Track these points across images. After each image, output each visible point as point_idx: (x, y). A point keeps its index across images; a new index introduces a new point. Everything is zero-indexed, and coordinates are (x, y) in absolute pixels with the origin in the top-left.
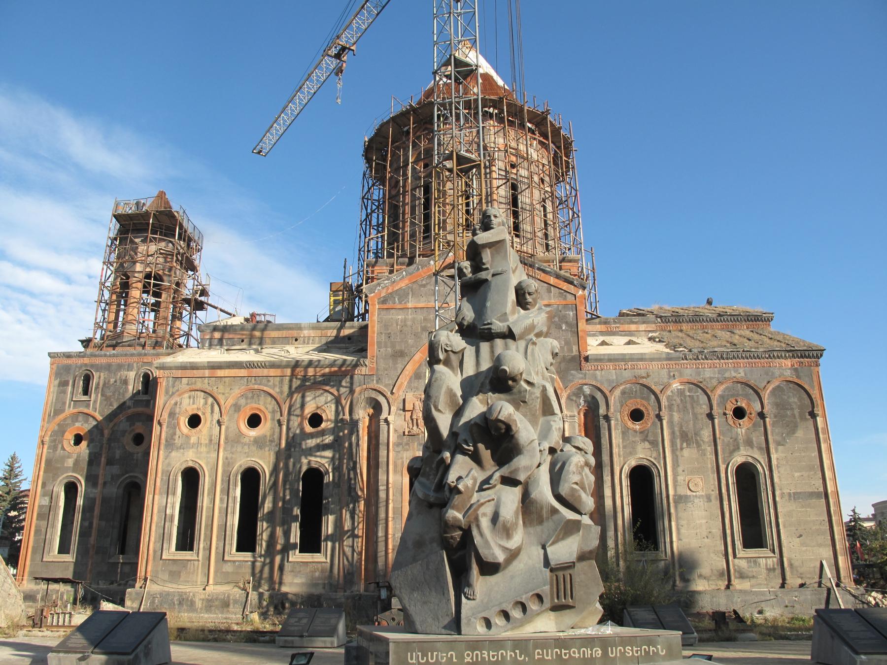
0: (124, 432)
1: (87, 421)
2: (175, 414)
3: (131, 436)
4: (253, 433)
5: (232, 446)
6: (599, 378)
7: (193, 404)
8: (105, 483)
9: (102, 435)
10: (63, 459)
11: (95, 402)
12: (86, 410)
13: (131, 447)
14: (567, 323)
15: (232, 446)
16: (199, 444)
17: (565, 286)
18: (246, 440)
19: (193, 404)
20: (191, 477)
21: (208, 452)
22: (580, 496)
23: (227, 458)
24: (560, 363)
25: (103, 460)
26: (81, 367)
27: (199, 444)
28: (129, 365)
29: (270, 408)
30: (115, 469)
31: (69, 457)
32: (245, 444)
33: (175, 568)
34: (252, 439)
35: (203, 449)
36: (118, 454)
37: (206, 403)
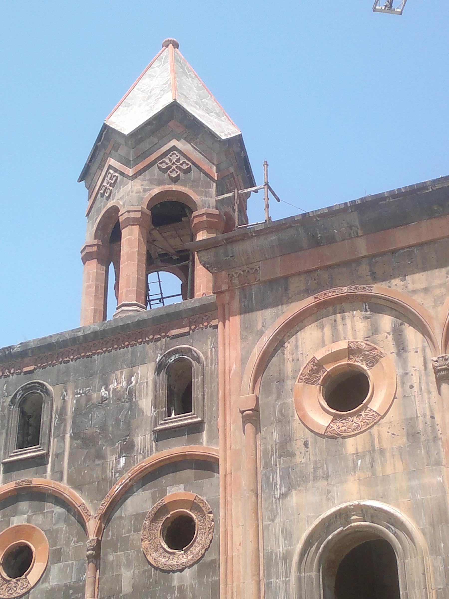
7: (335, 339)
11: (59, 456)
12: (37, 481)
21: (413, 473)
27: (374, 453)
35: (393, 467)
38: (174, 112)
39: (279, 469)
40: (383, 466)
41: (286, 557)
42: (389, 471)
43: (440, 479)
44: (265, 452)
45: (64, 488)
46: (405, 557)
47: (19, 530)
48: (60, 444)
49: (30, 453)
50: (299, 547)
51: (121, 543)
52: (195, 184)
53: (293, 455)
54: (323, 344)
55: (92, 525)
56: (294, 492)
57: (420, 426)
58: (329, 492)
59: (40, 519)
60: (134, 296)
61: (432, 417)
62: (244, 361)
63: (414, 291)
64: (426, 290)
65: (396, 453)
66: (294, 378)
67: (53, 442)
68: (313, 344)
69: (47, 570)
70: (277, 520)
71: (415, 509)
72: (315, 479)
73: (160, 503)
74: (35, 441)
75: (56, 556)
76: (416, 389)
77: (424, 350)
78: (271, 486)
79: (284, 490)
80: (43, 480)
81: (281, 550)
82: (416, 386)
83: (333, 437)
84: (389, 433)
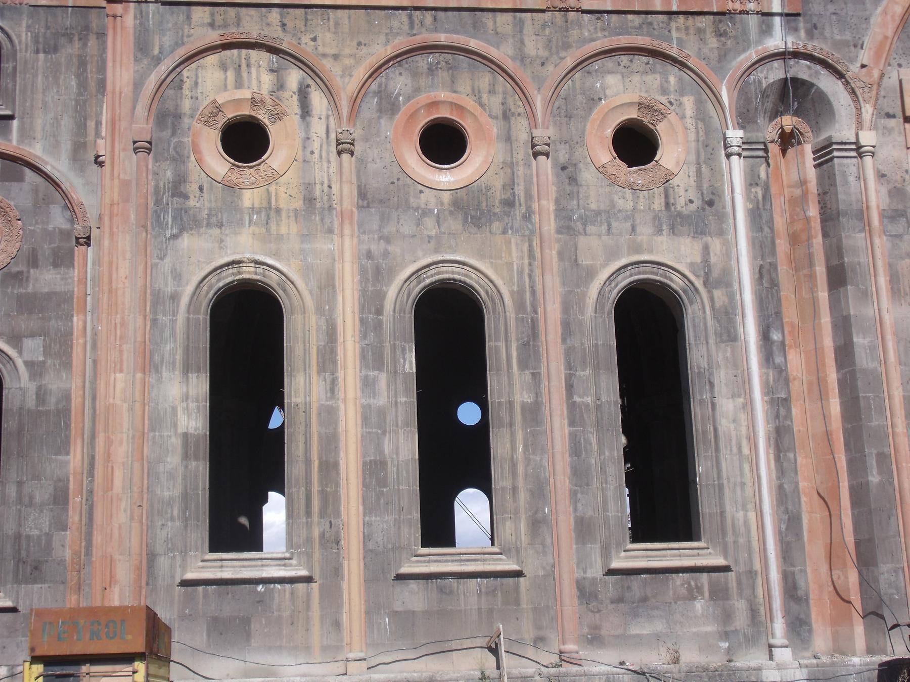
2: (178, 116)
4: (447, 178)
5: (384, 219)
7: (239, 85)
15: (384, 219)
18: (428, 197)
19: (239, 85)
21: (305, 237)
23: (369, 255)
29: (495, 103)
32: (426, 212)
33: (230, 606)
34: (446, 197)
35: (288, 228)
39: (171, 209)
40: (278, 225)
41: (175, 297)
42: (284, 230)
43: (331, 246)
44: (157, 187)
46: (292, 313)
50: (190, 289)
53: (186, 197)
56: (185, 235)
57: (318, 193)
58: (222, 241)
61: (330, 187)
62: (138, 85)
63: (324, 55)
64: (336, 57)
65: (292, 214)
66: (192, 117)
68: (220, 88)
70: (167, 260)
71: (307, 270)
72: (209, 225)
76: (316, 155)
77: (328, 117)
78: (160, 224)
79: (175, 231)
81: (170, 289)
82: (317, 152)
83: (231, 188)
84: (287, 195)
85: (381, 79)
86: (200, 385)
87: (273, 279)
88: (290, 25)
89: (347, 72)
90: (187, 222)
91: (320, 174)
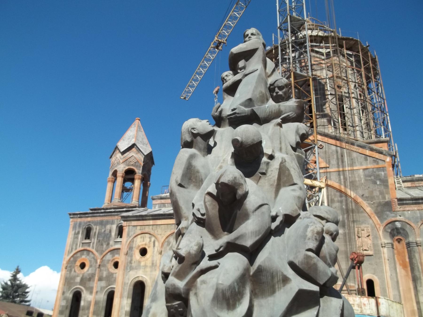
0: (109, 261)
1: (88, 255)
3: (113, 263)
6: (407, 216)
7: (143, 241)
8: (97, 292)
9: (96, 262)
10: (74, 278)
11: (93, 243)
12: (88, 248)
13: (112, 269)
14: (380, 180)
16: (145, 266)
17: (377, 155)
19: (143, 241)
20: (139, 288)
21: (151, 271)
22: (315, 265)
24: (377, 207)
25: (96, 278)
26: (87, 223)
28: (112, 221)
30: (103, 284)
31: (78, 276)
35: (148, 269)
36: (105, 274)
37: (150, 241)
38: (133, 146)
41: (128, 283)
45: (94, 251)
47: (83, 259)
48: (94, 240)
49: (87, 241)
51: (104, 266)
52: (137, 167)
54: (141, 242)
55: (99, 261)
57: (154, 262)
59: (88, 257)
60: (118, 196)
62: (127, 242)
64: (161, 235)
67: (93, 240)
69: (89, 269)
73: (113, 258)
74: (89, 238)
75: (91, 266)
78: (127, 269)
80: (90, 248)
84: (149, 263)
85: (168, 239)
86: (130, 301)
87: (144, 280)
88: (153, 228)
89: (162, 237)
90: (131, 269)
91: (155, 259)
